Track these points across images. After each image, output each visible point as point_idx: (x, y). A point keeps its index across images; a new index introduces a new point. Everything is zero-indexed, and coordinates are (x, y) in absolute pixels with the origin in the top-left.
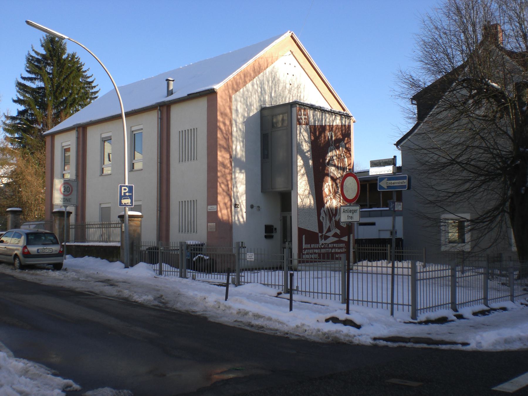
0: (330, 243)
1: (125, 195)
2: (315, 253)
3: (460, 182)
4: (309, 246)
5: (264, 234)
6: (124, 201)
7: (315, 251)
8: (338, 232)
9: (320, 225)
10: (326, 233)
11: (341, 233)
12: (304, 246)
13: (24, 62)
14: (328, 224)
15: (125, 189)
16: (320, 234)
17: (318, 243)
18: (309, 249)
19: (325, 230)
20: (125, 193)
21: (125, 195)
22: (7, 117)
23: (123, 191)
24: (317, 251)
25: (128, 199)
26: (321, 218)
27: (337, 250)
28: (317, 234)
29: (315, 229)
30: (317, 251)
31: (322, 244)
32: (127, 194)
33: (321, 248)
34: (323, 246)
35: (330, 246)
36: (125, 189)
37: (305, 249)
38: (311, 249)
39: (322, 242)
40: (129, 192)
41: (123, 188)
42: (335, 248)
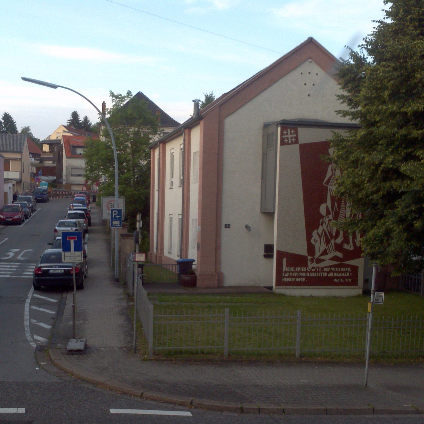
0: (326, 267)
1: (115, 218)
2: (302, 277)
3: (330, 231)
4: (292, 269)
5: (263, 253)
6: (114, 223)
7: (301, 274)
8: (340, 255)
9: (311, 249)
10: (320, 256)
11: (344, 256)
12: (284, 269)
13: (26, 126)
14: (323, 247)
15: (115, 213)
16: (309, 258)
17: (306, 266)
18: (292, 272)
19: (317, 254)
20: (115, 216)
21: (115, 218)
22: (68, 120)
23: (114, 214)
24: (304, 274)
25: (117, 220)
26: (312, 241)
27: (336, 274)
28: (305, 258)
29: (302, 251)
30: (304, 274)
31: (313, 268)
32: (117, 217)
33: (311, 271)
34: (313, 270)
35: (325, 269)
36: (115, 213)
37: (286, 272)
38: (295, 272)
39: (310, 265)
40: (118, 215)
41: (114, 211)
42: (334, 272)
